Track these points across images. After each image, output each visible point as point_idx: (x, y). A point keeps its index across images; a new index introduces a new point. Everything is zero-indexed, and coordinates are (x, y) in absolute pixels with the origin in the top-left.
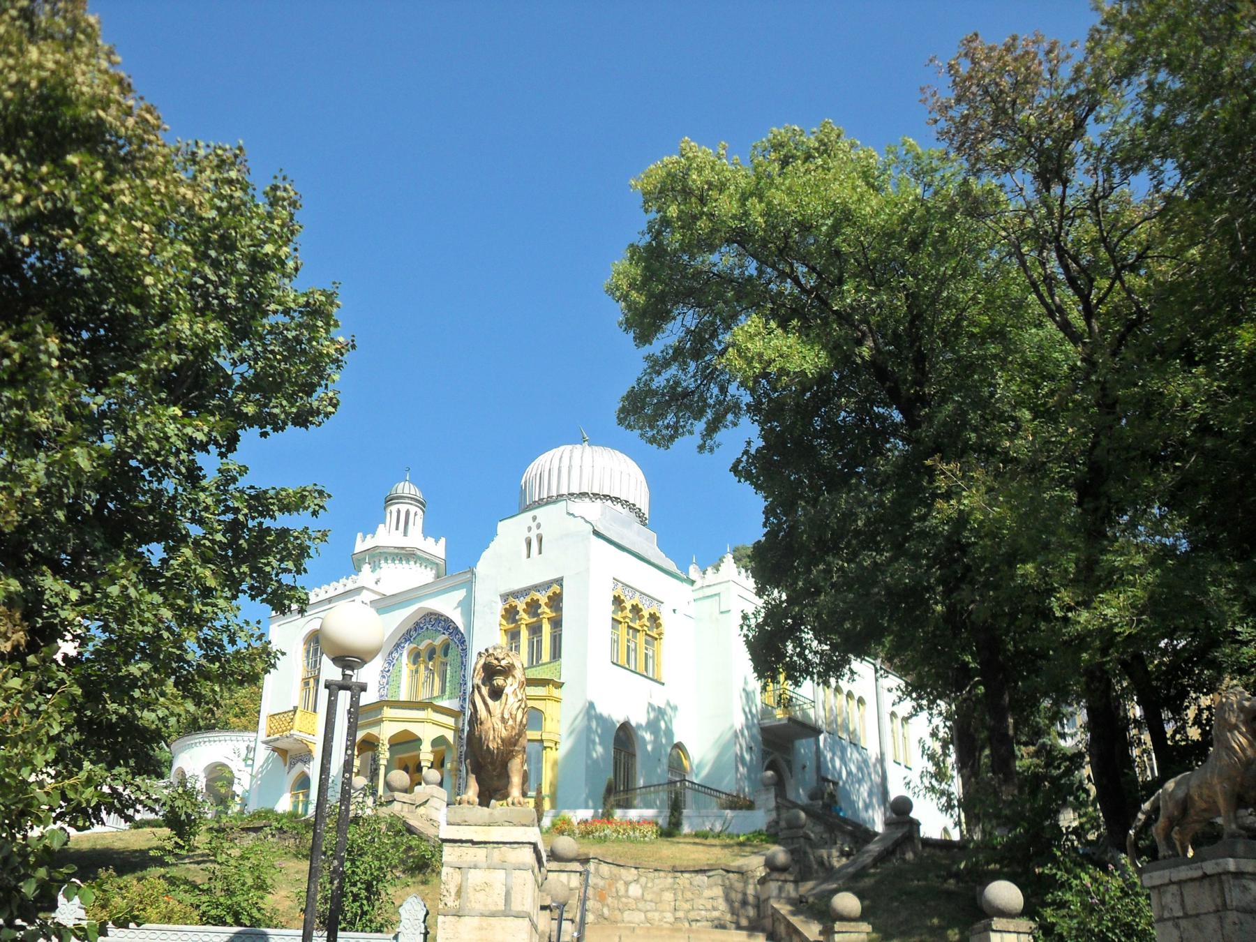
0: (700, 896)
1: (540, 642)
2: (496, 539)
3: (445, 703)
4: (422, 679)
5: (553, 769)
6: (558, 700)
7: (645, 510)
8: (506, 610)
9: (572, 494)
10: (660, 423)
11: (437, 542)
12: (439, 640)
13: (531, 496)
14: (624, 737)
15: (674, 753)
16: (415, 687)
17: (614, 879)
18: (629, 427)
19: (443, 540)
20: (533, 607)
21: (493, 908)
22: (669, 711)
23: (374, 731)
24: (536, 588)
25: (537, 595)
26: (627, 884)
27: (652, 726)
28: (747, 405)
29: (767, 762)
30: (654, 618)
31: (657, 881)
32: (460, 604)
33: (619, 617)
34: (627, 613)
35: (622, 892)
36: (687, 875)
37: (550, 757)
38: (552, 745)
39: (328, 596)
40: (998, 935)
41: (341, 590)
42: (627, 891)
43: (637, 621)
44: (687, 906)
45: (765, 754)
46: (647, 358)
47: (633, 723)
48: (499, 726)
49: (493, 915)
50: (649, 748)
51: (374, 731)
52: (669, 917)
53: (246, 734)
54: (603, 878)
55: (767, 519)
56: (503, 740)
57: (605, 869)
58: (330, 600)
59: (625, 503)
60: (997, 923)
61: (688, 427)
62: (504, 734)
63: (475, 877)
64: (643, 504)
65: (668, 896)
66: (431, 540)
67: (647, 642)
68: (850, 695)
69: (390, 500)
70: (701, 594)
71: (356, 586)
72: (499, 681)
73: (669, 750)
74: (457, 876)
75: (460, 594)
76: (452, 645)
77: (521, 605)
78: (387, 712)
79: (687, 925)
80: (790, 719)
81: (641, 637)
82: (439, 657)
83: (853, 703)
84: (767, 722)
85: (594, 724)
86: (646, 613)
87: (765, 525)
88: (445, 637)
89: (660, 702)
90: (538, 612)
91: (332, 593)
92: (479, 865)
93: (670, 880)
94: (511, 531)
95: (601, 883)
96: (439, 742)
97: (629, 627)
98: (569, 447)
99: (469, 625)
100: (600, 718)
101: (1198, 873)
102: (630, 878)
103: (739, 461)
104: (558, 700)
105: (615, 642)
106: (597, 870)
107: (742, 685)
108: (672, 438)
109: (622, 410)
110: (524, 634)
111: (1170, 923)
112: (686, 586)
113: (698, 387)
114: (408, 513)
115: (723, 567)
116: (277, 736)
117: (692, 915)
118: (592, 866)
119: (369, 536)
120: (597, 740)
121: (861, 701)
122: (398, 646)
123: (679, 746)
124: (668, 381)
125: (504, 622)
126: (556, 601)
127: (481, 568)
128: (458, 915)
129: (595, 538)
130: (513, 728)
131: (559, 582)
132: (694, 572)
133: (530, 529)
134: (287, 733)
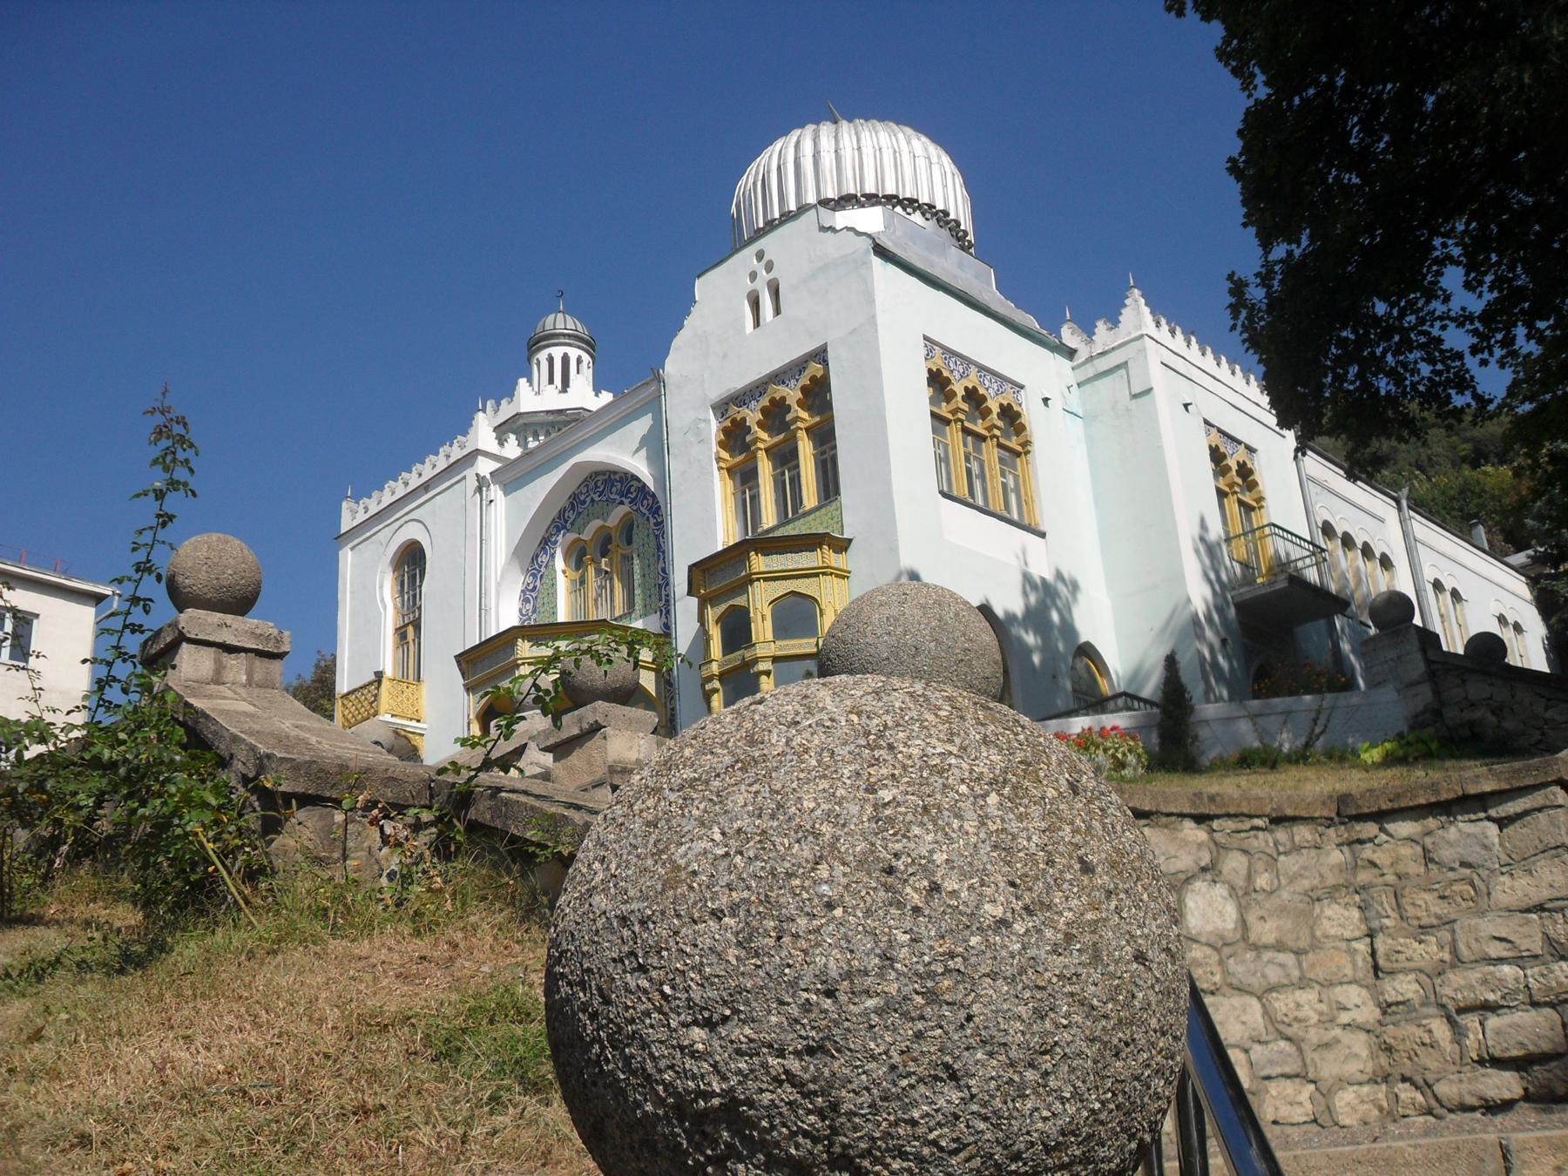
0: (1480, 900)
2: (695, 311)
4: (592, 594)
7: (966, 224)
8: (725, 431)
9: (824, 203)
13: (750, 222)
20: (776, 415)
24: (778, 377)
25: (781, 391)
30: (1010, 415)
31: (1288, 863)
32: (644, 442)
33: (944, 410)
34: (959, 402)
36: (1404, 828)
41: (442, 463)
43: (980, 426)
44: (1429, 951)
52: (1359, 1004)
58: (426, 487)
59: (928, 210)
64: (960, 210)
65: (1340, 919)
67: (1001, 460)
68: (1367, 551)
69: (537, 343)
70: (1089, 371)
71: (465, 452)
75: (642, 425)
77: (752, 416)
79: (1441, 1030)
81: (991, 453)
82: (618, 551)
83: (1374, 567)
86: (993, 405)
88: (625, 509)
89: (1042, 570)
90: (786, 423)
93: (1337, 857)
94: (719, 292)
98: (810, 128)
102: (1184, 862)
104: (843, 575)
105: (942, 460)
107: (1196, 531)
110: (765, 468)
114: (565, 359)
115: (1127, 315)
117: (1461, 985)
119: (504, 402)
123: (1087, 652)
125: (725, 455)
127: (673, 367)
129: (877, 262)
131: (820, 355)
132: (1069, 336)
133: (753, 276)
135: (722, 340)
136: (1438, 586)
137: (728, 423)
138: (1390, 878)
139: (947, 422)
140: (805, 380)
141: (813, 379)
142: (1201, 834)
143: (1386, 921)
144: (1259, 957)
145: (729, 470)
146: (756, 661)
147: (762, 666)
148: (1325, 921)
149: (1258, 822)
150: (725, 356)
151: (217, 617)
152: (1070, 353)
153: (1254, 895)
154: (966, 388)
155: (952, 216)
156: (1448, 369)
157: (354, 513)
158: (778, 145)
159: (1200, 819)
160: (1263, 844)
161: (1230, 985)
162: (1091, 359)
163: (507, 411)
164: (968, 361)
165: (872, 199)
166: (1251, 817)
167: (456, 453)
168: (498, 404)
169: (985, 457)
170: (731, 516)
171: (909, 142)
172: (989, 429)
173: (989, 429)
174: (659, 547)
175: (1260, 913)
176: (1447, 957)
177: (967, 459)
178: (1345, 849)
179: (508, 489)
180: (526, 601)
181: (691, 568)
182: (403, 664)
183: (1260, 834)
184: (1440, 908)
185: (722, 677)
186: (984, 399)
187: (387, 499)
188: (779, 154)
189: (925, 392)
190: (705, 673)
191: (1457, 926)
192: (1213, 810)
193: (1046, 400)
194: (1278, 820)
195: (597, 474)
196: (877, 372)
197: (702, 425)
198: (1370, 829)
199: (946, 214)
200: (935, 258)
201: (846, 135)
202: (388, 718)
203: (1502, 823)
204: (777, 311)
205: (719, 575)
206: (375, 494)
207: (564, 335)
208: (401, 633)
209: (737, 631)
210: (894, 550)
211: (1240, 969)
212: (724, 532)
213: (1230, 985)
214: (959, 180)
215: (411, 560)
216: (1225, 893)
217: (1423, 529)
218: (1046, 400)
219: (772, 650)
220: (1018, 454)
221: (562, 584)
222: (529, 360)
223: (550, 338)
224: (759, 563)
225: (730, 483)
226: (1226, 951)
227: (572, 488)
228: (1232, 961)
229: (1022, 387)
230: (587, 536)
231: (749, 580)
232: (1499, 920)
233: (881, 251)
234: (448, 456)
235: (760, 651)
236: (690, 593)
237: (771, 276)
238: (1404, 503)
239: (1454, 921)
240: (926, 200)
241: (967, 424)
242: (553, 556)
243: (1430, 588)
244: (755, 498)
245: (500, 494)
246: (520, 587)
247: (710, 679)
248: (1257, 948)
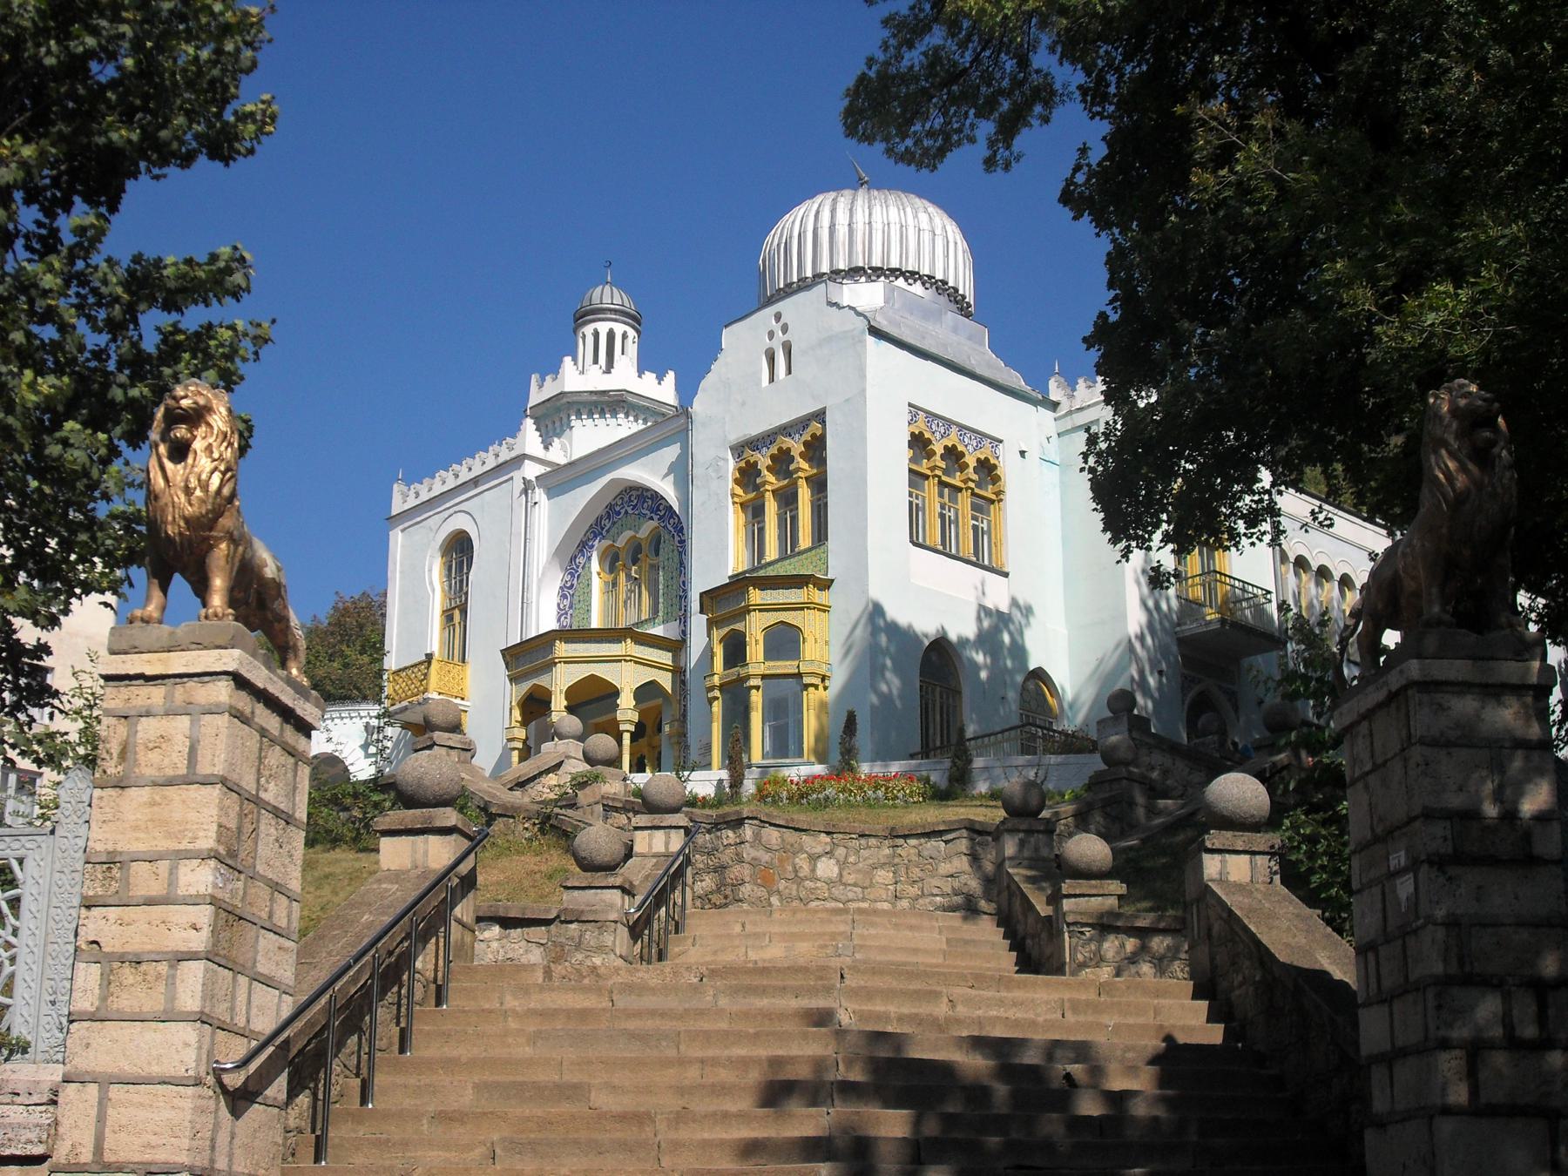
0: (933, 873)
1: (794, 519)
3: (658, 630)
4: (622, 597)
5: (818, 717)
6: (824, 609)
7: (966, 287)
8: (740, 470)
9: (836, 272)
10: (917, 127)
11: (660, 379)
12: (647, 528)
14: (939, 658)
15: (1031, 686)
16: (610, 609)
17: (790, 851)
18: (868, 138)
19: (671, 376)
20: (782, 462)
21: (170, 772)
22: (1017, 615)
23: (542, 681)
26: (814, 858)
27: (987, 640)
28: (1080, 87)
29: (1191, 694)
30: (987, 469)
32: (672, 469)
33: (924, 467)
35: (805, 869)
36: (913, 842)
37: (812, 698)
38: (817, 681)
39: (472, 475)
40: (1217, 857)
41: (491, 463)
42: (813, 870)
44: (914, 891)
45: (1187, 682)
46: (886, 22)
47: (953, 636)
48: (182, 498)
49: (170, 783)
50: (983, 675)
51: (542, 681)
53: (363, 706)
54: (769, 850)
55: (1112, 272)
56: (187, 520)
57: (772, 835)
58: (475, 482)
59: (928, 281)
60: (1214, 838)
61: (967, 131)
62: (189, 511)
63: (148, 729)
65: (884, 876)
66: (650, 377)
67: (975, 507)
69: (583, 316)
70: (1068, 424)
72: (181, 432)
73: (1020, 679)
74: (122, 730)
75: (671, 453)
77: (763, 460)
78: (562, 649)
80: (1223, 621)
81: (965, 500)
82: (647, 560)
84: (1190, 628)
85: (883, 639)
86: (971, 461)
87: (1111, 285)
88: (653, 524)
90: (790, 467)
91: (478, 470)
92: (154, 711)
93: (887, 851)
94: (743, 343)
95: (766, 857)
96: (646, 692)
97: (942, 484)
98: (832, 195)
99: (686, 500)
100: (893, 629)
101: (1380, 696)
102: (819, 849)
103: (1070, 182)
104: (824, 609)
105: (914, 511)
106: (757, 836)
108: (941, 153)
109: (849, 112)
110: (771, 507)
111: (1360, 785)
112: (1046, 415)
113: (976, 59)
116: (405, 703)
118: (748, 831)
119: (548, 378)
120: (889, 663)
123: (1040, 675)
124: (925, 54)
125: (739, 491)
126: (816, 449)
128: (121, 786)
129: (871, 340)
130: (202, 501)
131: (820, 416)
133: (771, 335)
134: (420, 697)
135: (744, 390)
137: (743, 464)
139: (927, 477)
140: (807, 437)
141: (813, 436)
142: (828, 839)
145: (741, 504)
146: (748, 677)
147: (753, 682)
150: (743, 404)
151: (447, 735)
152: (1054, 406)
154: (946, 447)
155: (951, 284)
156: (1261, 501)
157: (405, 496)
158: (799, 211)
159: (828, 833)
162: (1070, 413)
163: (550, 389)
164: (949, 423)
165: (878, 272)
167: (505, 455)
168: (543, 380)
169: (959, 506)
170: (742, 544)
171: (916, 216)
172: (965, 482)
173: (965, 482)
174: (681, 563)
177: (943, 507)
179: (552, 493)
180: (564, 597)
181: (702, 595)
182: (448, 645)
184: (920, 874)
185: (722, 687)
187: (438, 489)
188: (801, 220)
189: (906, 453)
190: (708, 684)
194: (862, 836)
195: (631, 489)
196: (864, 438)
197: (721, 463)
198: (901, 841)
199: (945, 283)
200: (930, 326)
201: (859, 210)
202: (435, 696)
203: (946, 842)
204: (789, 371)
205: (726, 601)
206: (427, 481)
207: (611, 310)
208: (448, 616)
209: (736, 650)
210: (865, 591)
212: (735, 560)
214: (962, 245)
215: (459, 549)
218: (1022, 453)
219: (762, 670)
220: (992, 502)
221: (597, 584)
222: (575, 331)
223: (596, 313)
224: (756, 596)
225: (742, 516)
227: (609, 499)
230: (621, 542)
231: (747, 610)
233: (875, 332)
234: (497, 456)
235: (752, 670)
236: (701, 612)
237: (785, 338)
240: (927, 272)
241: (944, 478)
242: (589, 558)
244: (761, 530)
245: (544, 497)
246: (558, 584)
247: (711, 689)
248: (845, 885)
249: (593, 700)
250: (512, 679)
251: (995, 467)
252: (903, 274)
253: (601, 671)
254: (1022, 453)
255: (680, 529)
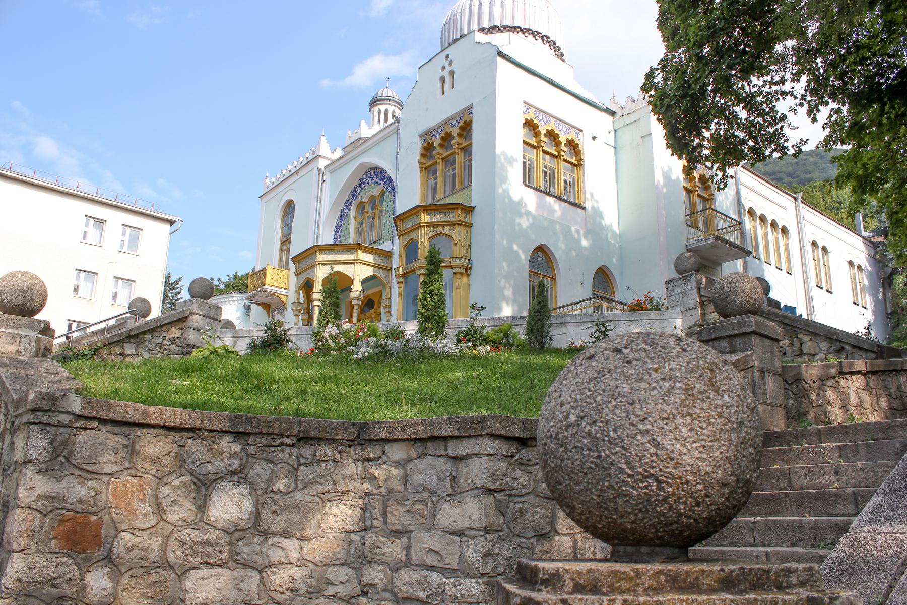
0: (429, 523)
38: (463, 271)
58: (297, 172)
76: (386, 191)
102: (218, 465)
112: (610, 118)
114: (387, 112)
121: (784, 231)
122: (348, 203)
125: (423, 161)
126: (466, 128)
129: (499, 60)
131: (468, 110)
133: (443, 68)
136: (814, 244)
138: (383, 490)
141: (465, 122)
142: (237, 448)
143: (375, 523)
144: (265, 541)
148: (331, 518)
149: (288, 441)
153: (272, 495)
154: (547, 130)
159: (238, 435)
160: (286, 455)
161: (236, 561)
166: (282, 436)
175: (274, 508)
176: (403, 558)
178: (360, 464)
180: (337, 232)
183: (287, 449)
186: (558, 136)
191: (413, 534)
192: (249, 429)
193: (594, 138)
194: (304, 439)
195: (371, 169)
208: (283, 243)
211: (246, 549)
213: (236, 561)
216: (246, 492)
217: (808, 213)
226: (237, 534)
228: (240, 543)
229: (581, 131)
231: (419, 227)
232: (437, 537)
238: (800, 200)
239: (412, 531)
243: (809, 247)
246: (335, 225)
249: (337, 287)
250: (297, 274)
251: (578, 145)
252: (522, 30)
253: (337, 268)
254: (594, 138)
255: (394, 189)
